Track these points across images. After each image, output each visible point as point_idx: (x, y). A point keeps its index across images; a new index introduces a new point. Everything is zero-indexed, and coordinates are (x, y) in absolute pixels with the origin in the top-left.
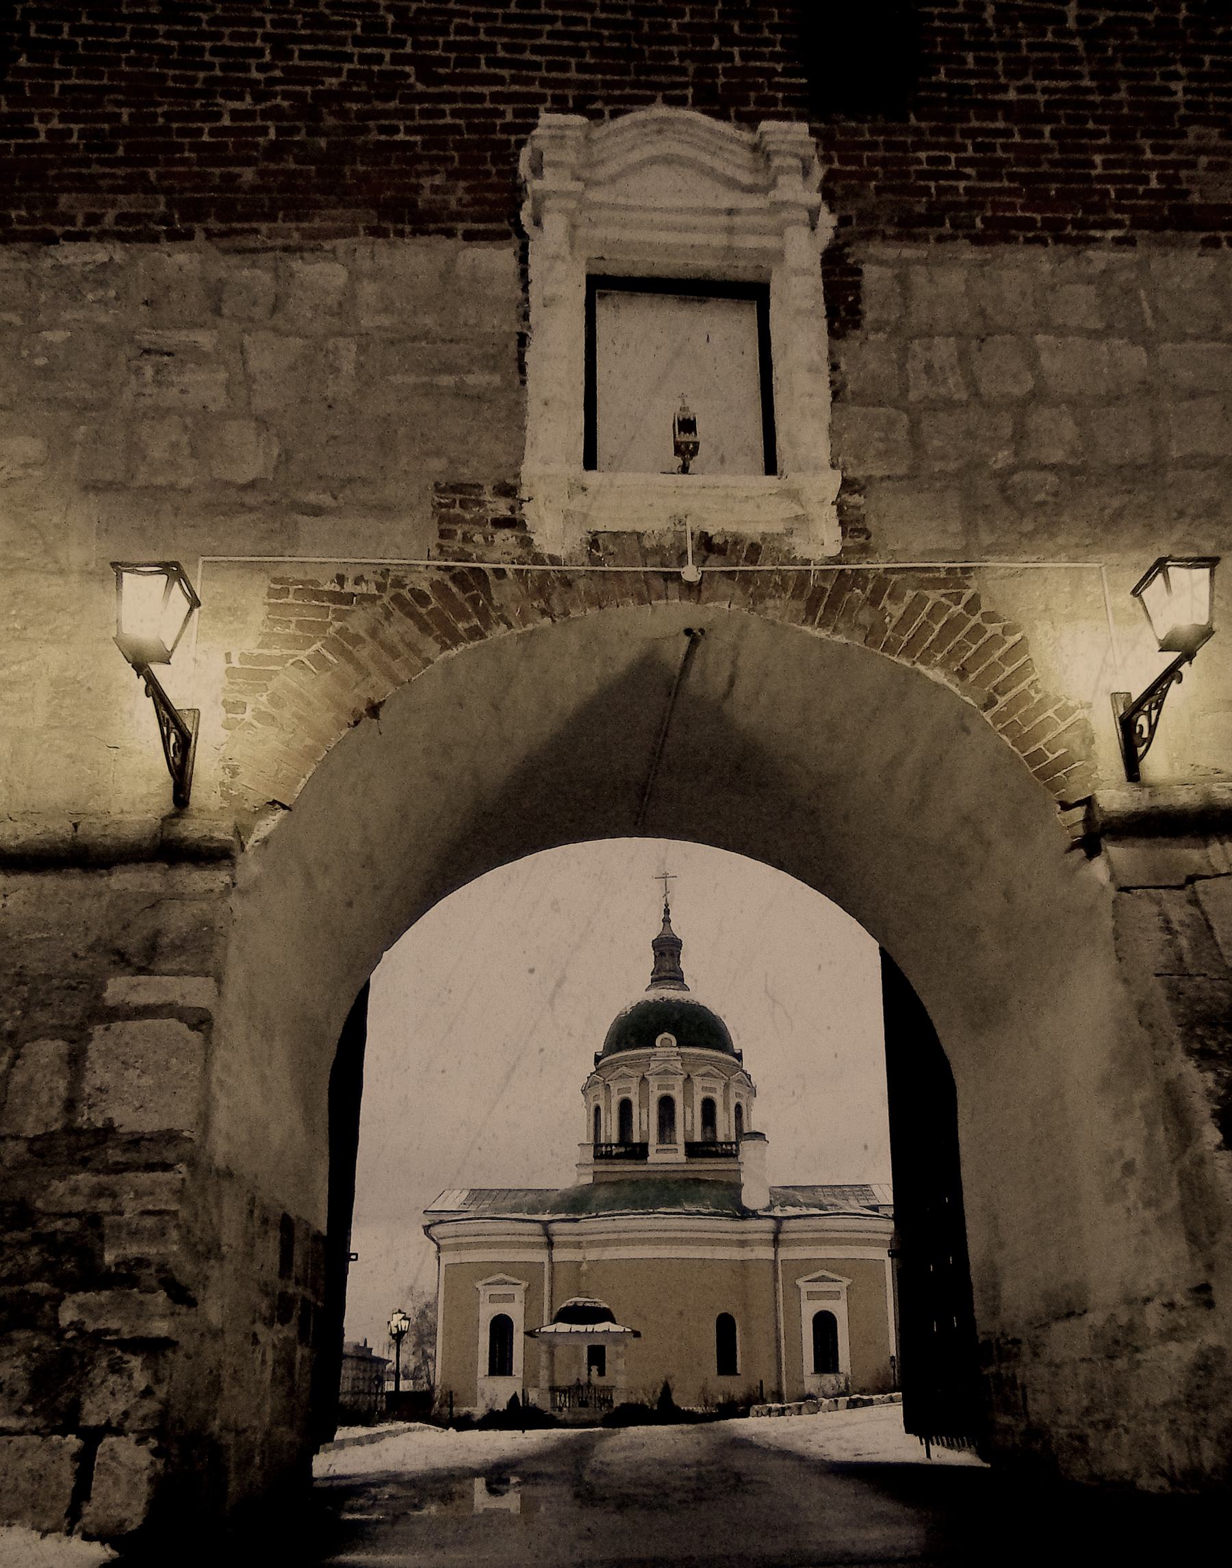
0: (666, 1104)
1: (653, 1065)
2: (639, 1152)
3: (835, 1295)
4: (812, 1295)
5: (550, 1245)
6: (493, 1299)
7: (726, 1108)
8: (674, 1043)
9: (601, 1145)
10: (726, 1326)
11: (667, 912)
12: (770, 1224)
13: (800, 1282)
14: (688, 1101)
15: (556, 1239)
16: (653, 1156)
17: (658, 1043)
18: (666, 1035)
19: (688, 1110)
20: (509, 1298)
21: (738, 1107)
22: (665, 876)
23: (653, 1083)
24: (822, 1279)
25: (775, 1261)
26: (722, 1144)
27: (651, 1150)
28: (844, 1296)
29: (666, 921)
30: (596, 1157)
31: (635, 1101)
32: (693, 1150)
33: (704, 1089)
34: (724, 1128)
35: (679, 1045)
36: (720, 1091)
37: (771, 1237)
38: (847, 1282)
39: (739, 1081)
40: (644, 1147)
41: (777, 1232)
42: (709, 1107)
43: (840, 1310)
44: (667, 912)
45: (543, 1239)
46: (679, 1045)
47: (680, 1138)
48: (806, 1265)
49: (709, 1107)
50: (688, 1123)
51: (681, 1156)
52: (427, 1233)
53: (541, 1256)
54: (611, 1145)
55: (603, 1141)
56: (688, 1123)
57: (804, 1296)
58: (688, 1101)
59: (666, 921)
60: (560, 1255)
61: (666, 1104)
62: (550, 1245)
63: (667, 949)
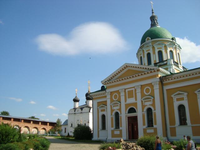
0: (149, 55)
13: (173, 96)
14: (154, 53)
18: (148, 38)
24: (179, 94)
31: (142, 56)
33: (158, 48)
35: (151, 39)
38: (186, 94)
44: (152, 11)
46: (151, 39)
47: (153, 62)
49: (160, 53)
50: (155, 58)
56: (155, 58)
61: (149, 55)
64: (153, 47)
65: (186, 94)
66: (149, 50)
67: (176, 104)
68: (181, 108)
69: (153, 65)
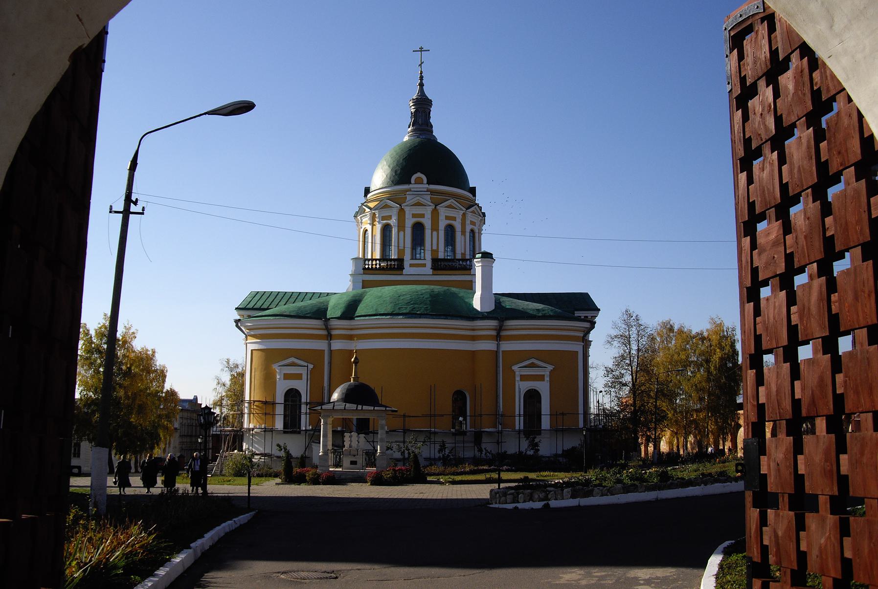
0: (418, 228)
1: (408, 197)
2: (398, 266)
3: (541, 378)
4: (523, 378)
5: (329, 337)
6: (287, 377)
7: (463, 232)
8: (425, 180)
9: (369, 260)
10: (459, 397)
11: (421, 78)
12: (493, 323)
14: (435, 228)
15: (334, 332)
16: (407, 270)
17: (413, 180)
18: (419, 175)
19: (435, 233)
20: (298, 377)
21: (472, 231)
22: (421, 50)
23: (409, 211)
25: (497, 352)
26: (459, 260)
27: (406, 264)
28: (547, 379)
29: (421, 85)
30: (364, 269)
32: (438, 265)
33: (447, 218)
34: (462, 245)
35: (428, 183)
36: (459, 220)
37: (494, 333)
38: (550, 367)
39: (473, 212)
40: (400, 261)
41: (499, 329)
42: (450, 231)
43: (544, 388)
44: (421, 78)
45: (324, 332)
46: (428, 183)
48: (521, 356)
49: (450, 231)
50: (434, 241)
51: (428, 269)
52: (237, 326)
53: (321, 345)
54: (376, 260)
55: (370, 257)
56: (434, 241)
57: (518, 378)
58: (435, 228)
59: (421, 85)
60: (337, 345)
61: (418, 228)
62: (329, 337)
63: (423, 105)
64: (435, 214)
65: (550, 367)
66: (423, 216)
67: (523, 387)
68: (532, 397)
69: (429, 263)
